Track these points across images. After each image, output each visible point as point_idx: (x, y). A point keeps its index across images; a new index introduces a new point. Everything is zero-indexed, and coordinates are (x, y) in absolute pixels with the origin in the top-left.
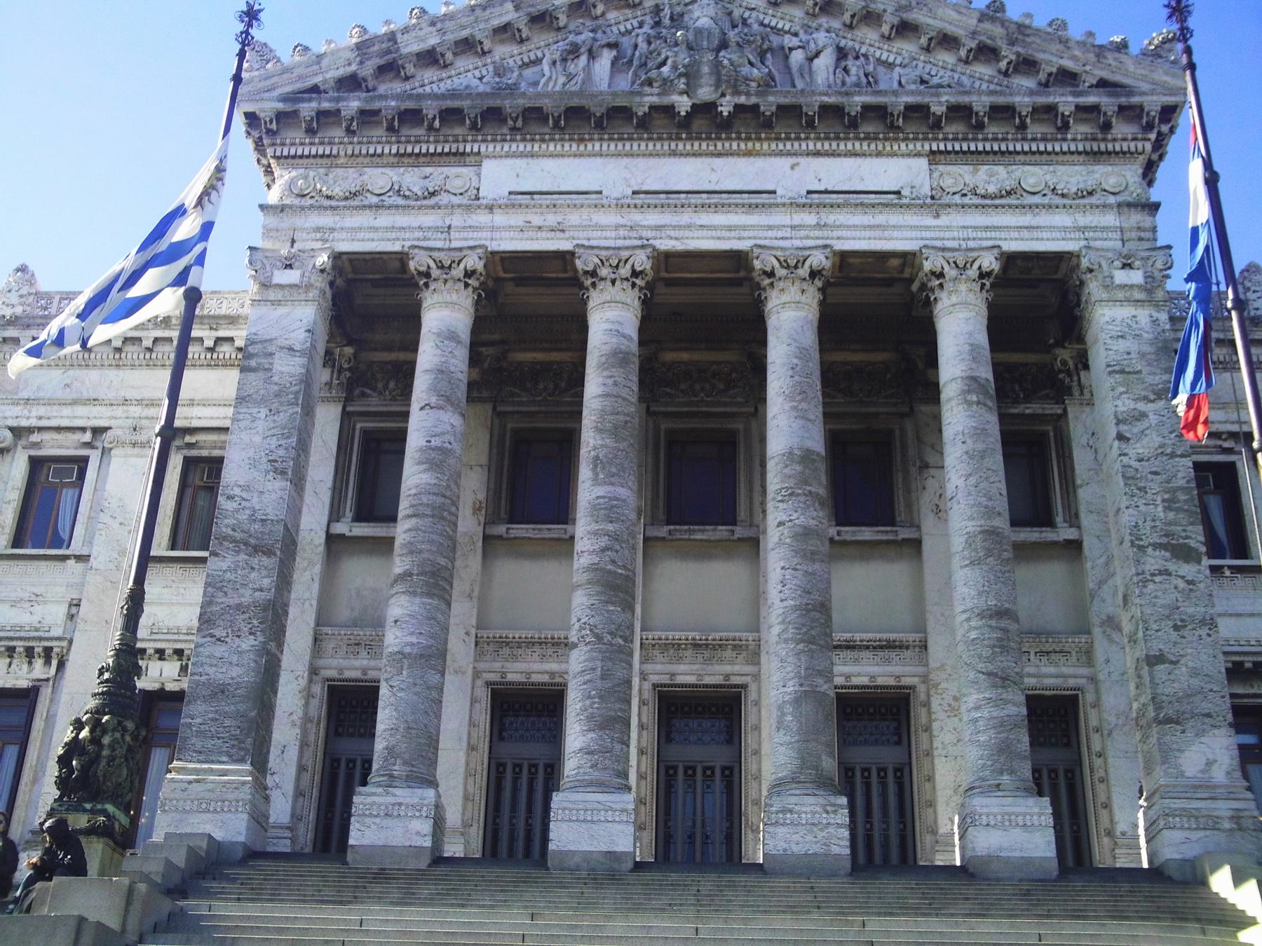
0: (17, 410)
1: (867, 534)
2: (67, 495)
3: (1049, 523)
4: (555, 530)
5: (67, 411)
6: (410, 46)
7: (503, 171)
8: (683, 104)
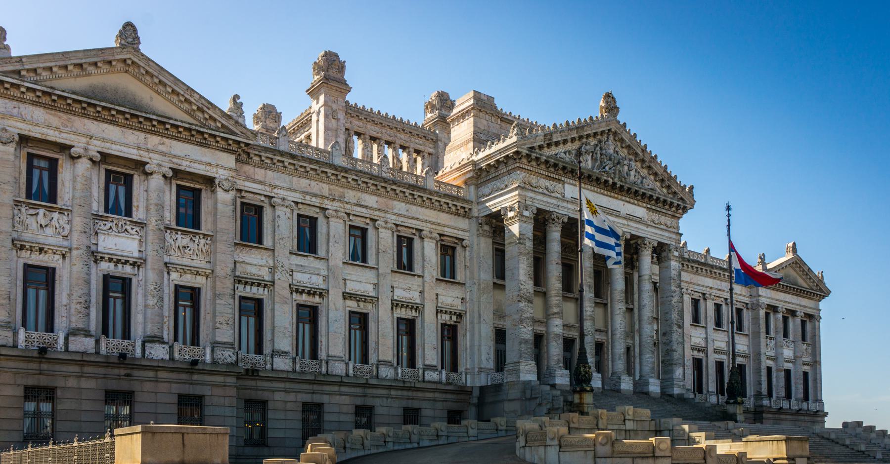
0: (394, 217)
5: (410, 221)
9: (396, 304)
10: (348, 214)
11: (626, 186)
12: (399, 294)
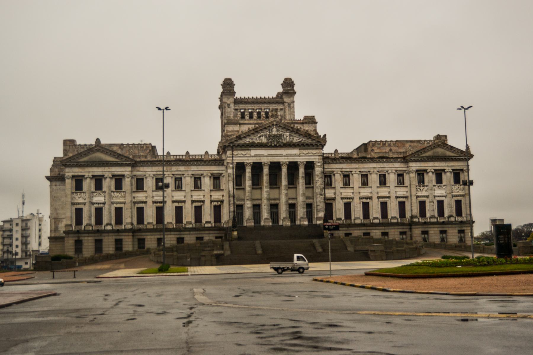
1: (291, 186)
2: (199, 182)
3: (310, 184)
4: (258, 187)
6: (242, 136)
7: (253, 152)
8: (273, 145)
9: (193, 202)
10: (173, 175)
11: (282, 145)
12: (194, 198)
